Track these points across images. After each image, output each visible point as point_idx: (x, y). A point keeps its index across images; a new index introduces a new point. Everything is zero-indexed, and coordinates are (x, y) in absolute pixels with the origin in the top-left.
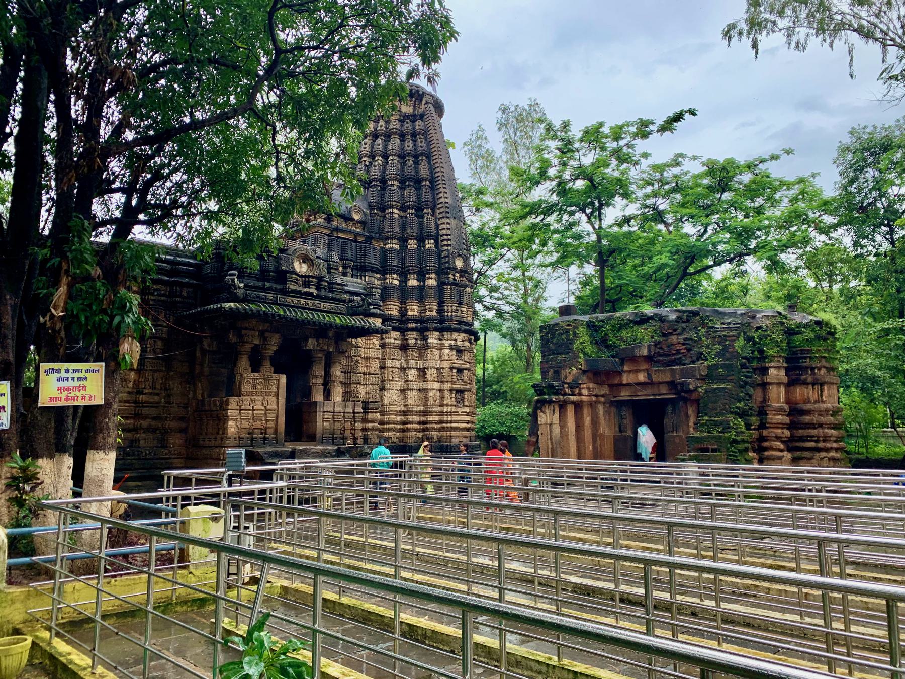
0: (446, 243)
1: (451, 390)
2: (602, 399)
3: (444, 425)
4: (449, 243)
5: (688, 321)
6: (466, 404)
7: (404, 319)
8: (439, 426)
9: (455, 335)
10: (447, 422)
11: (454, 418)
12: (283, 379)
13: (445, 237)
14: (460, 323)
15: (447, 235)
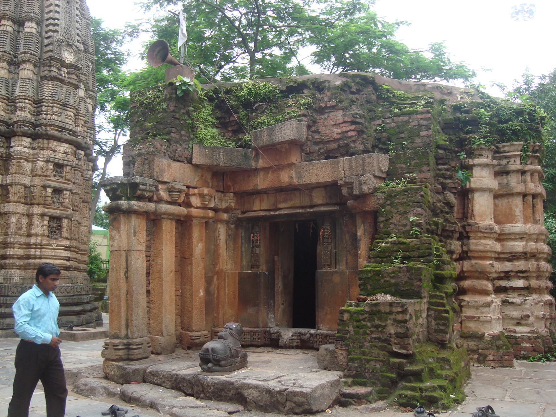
0: (51, 28)
1: (42, 216)
2: (225, 216)
3: (31, 261)
4: (56, 28)
5: (358, 91)
6: (65, 234)
8: (22, 262)
9: (53, 144)
10: (35, 257)
11: (46, 252)
13: (51, 21)
14: (62, 129)
15: (54, 19)
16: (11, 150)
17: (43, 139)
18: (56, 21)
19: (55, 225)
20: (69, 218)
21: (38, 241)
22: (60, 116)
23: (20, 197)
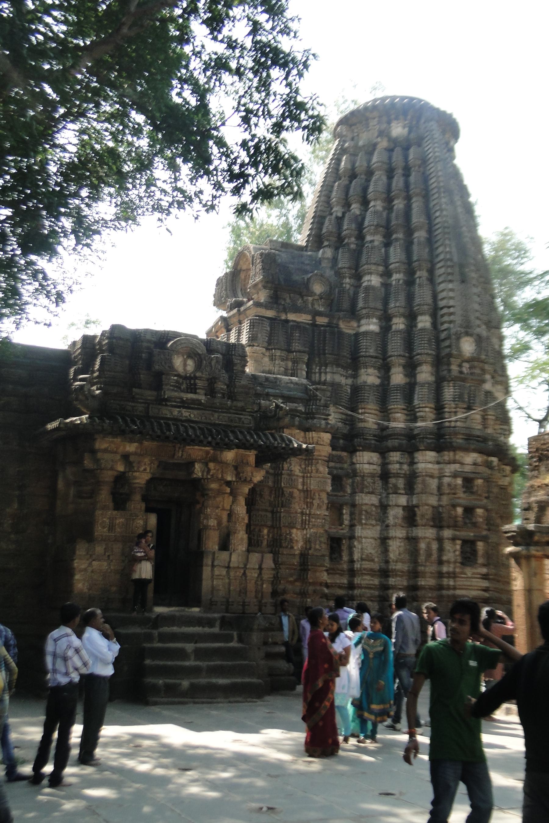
1: (453, 539)
4: (452, 318)
6: (480, 560)
7: (385, 433)
10: (448, 588)
12: (153, 519)
15: (449, 307)
16: (415, 466)
17: (449, 451)
18: (452, 310)
19: (468, 549)
20: (484, 539)
21: (451, 570)
22: (465, 422)
23: (427, 520)
